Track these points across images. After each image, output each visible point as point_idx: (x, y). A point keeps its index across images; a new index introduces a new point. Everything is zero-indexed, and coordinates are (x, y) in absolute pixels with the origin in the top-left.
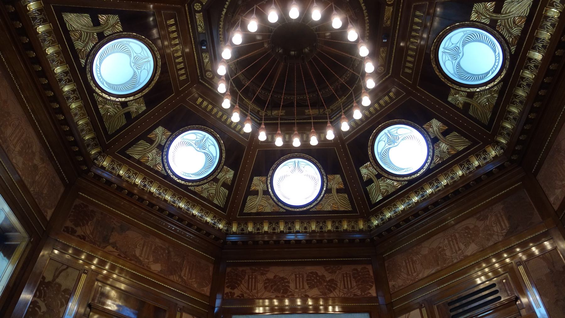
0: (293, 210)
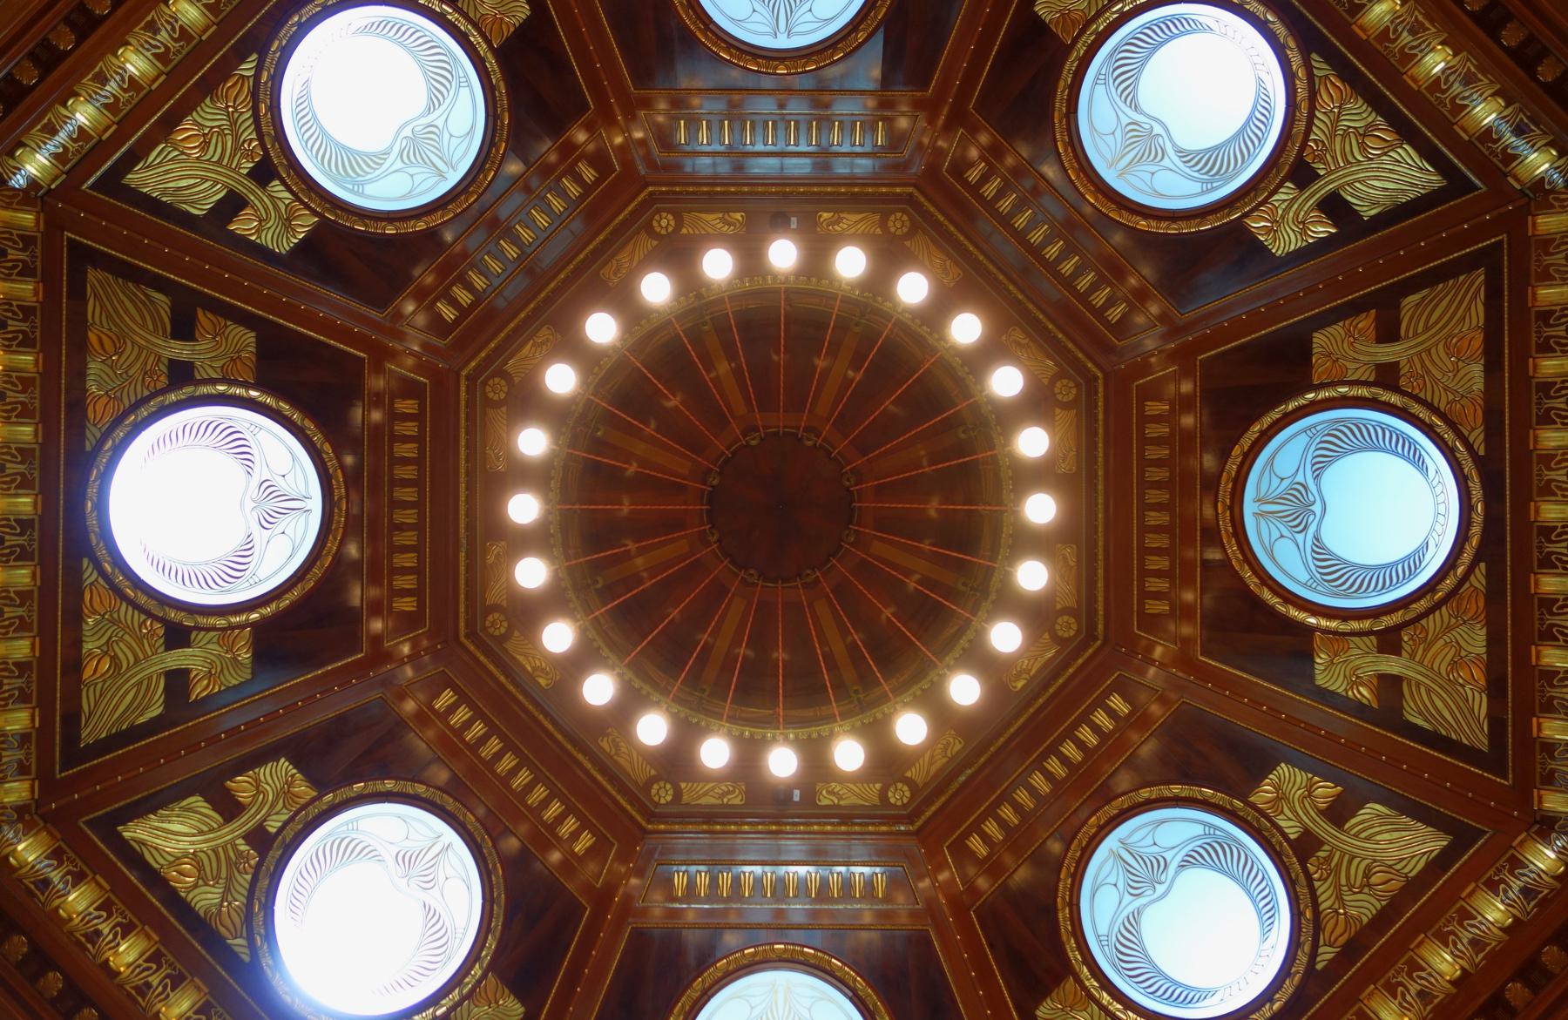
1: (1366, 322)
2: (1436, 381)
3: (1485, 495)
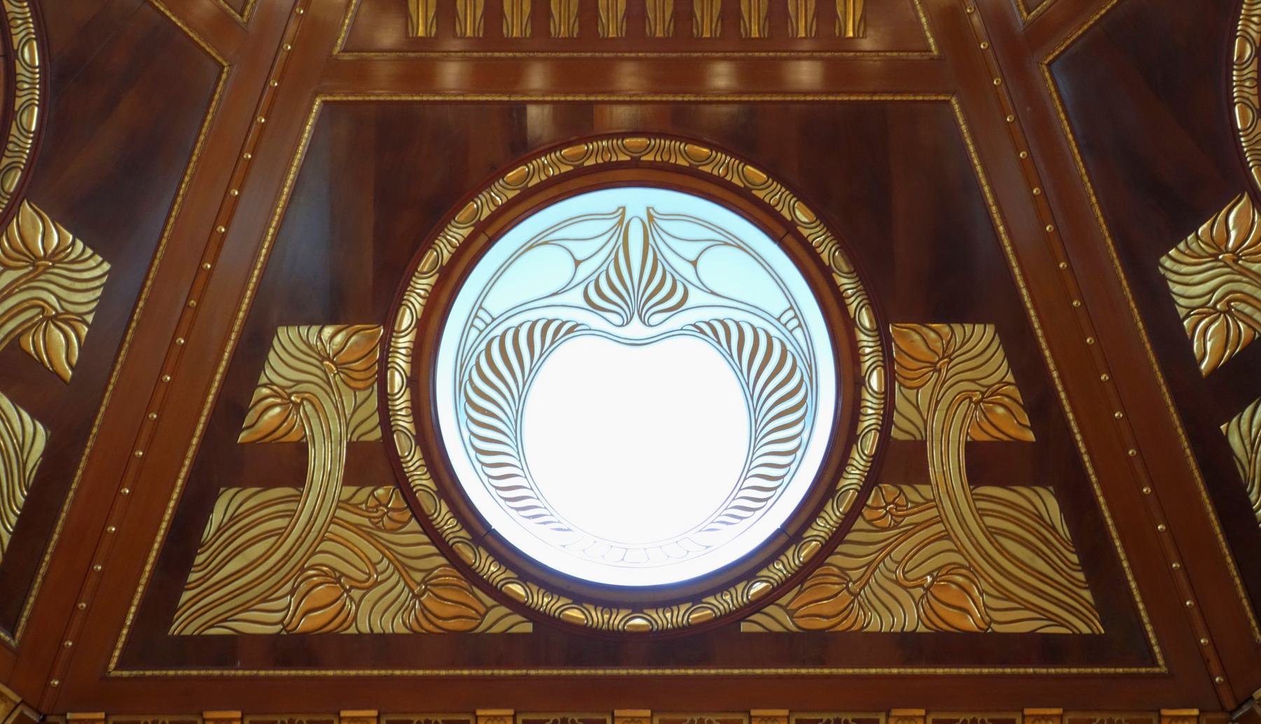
0: (597, 617)
1: (1013, 424)
2: (887, 548)
3: (664, 632)
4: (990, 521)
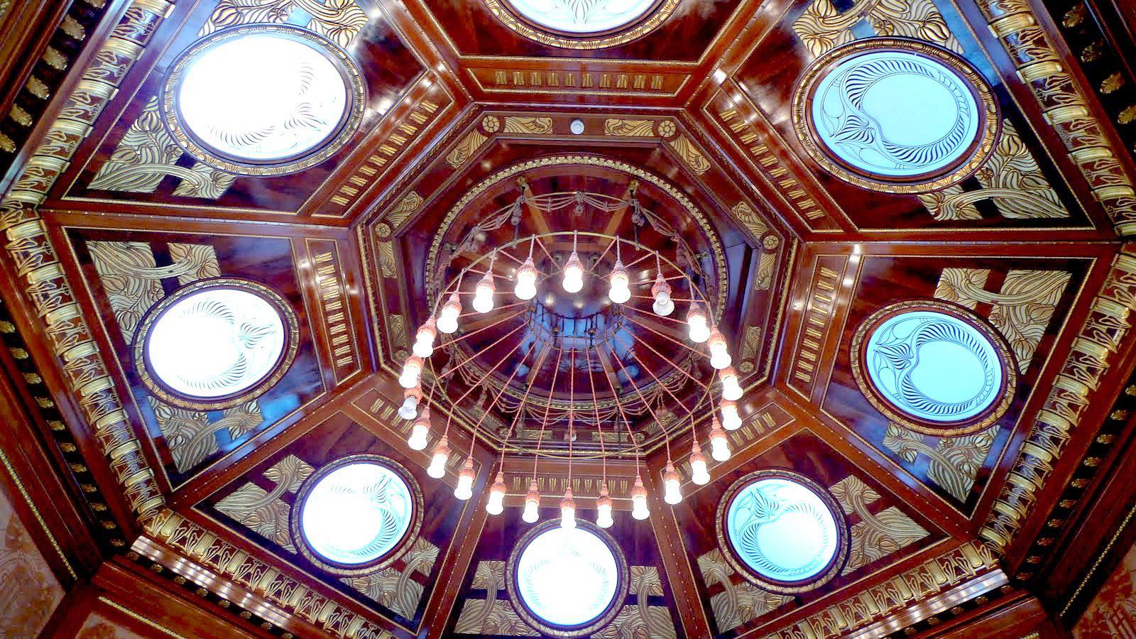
1: (981, 276)
4: (1015, 293)
